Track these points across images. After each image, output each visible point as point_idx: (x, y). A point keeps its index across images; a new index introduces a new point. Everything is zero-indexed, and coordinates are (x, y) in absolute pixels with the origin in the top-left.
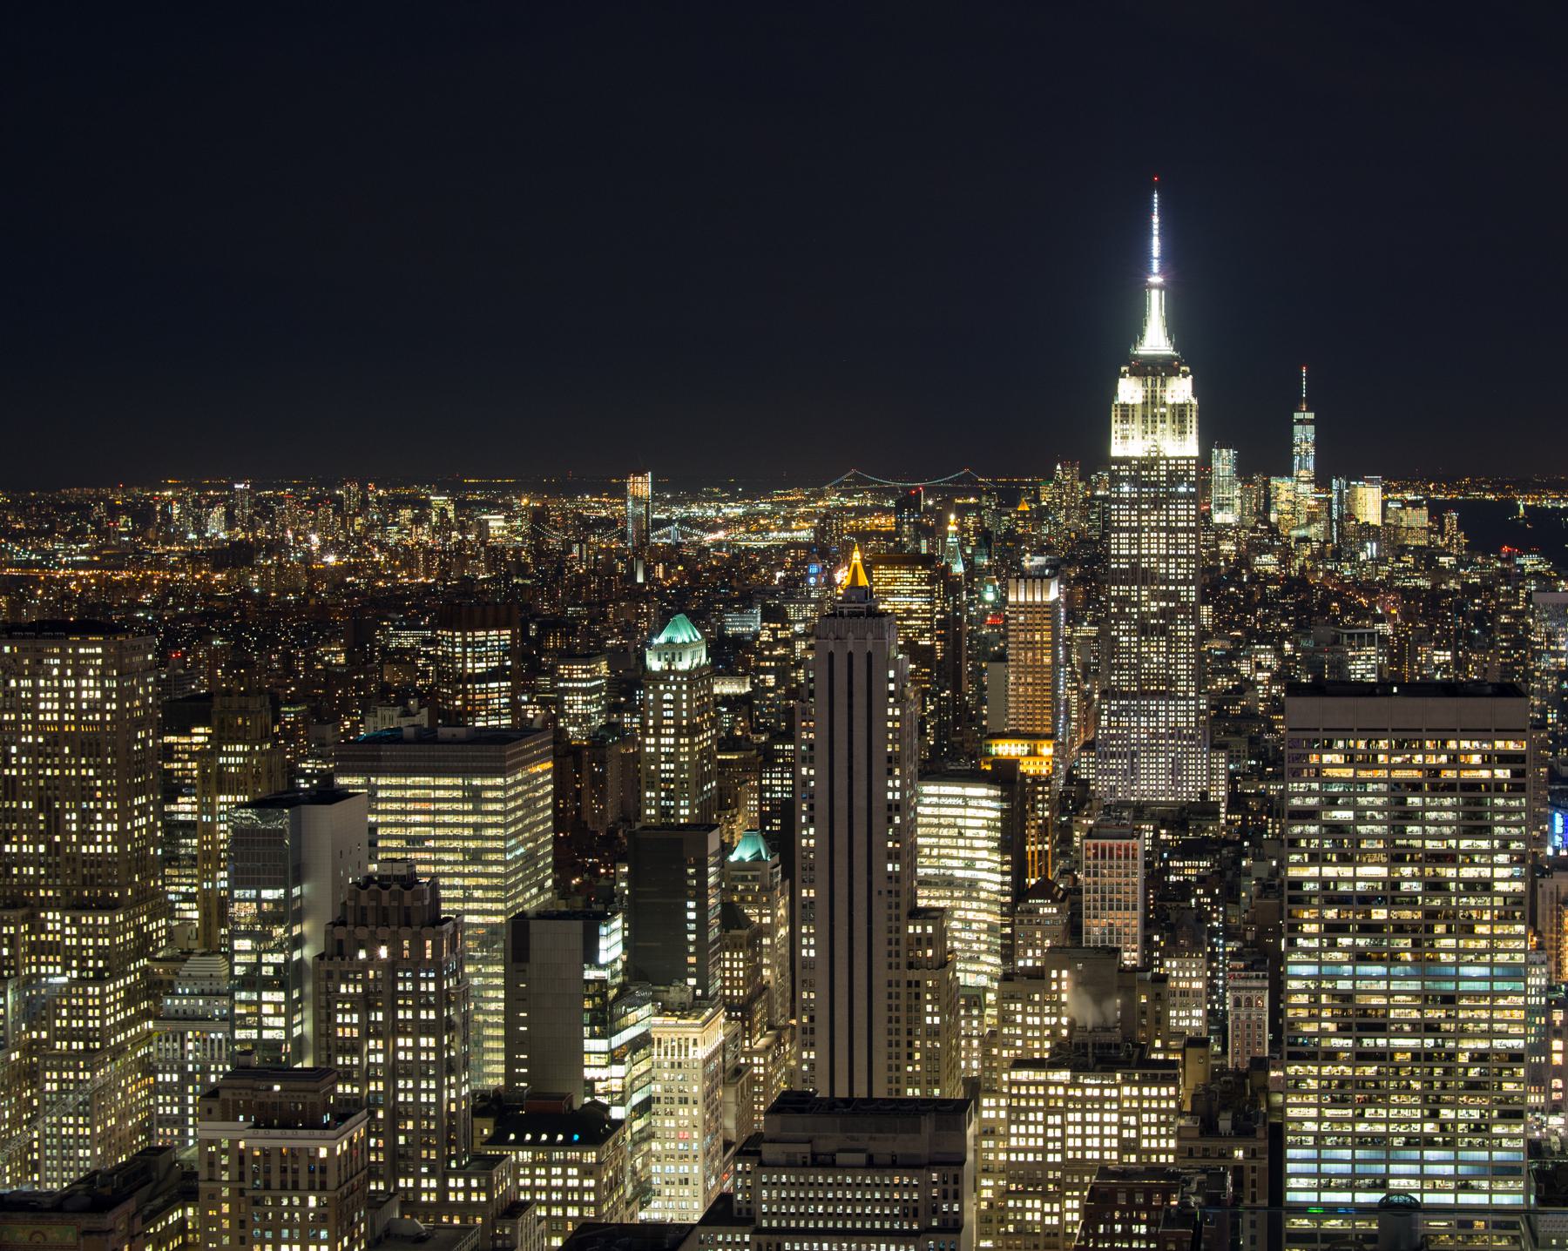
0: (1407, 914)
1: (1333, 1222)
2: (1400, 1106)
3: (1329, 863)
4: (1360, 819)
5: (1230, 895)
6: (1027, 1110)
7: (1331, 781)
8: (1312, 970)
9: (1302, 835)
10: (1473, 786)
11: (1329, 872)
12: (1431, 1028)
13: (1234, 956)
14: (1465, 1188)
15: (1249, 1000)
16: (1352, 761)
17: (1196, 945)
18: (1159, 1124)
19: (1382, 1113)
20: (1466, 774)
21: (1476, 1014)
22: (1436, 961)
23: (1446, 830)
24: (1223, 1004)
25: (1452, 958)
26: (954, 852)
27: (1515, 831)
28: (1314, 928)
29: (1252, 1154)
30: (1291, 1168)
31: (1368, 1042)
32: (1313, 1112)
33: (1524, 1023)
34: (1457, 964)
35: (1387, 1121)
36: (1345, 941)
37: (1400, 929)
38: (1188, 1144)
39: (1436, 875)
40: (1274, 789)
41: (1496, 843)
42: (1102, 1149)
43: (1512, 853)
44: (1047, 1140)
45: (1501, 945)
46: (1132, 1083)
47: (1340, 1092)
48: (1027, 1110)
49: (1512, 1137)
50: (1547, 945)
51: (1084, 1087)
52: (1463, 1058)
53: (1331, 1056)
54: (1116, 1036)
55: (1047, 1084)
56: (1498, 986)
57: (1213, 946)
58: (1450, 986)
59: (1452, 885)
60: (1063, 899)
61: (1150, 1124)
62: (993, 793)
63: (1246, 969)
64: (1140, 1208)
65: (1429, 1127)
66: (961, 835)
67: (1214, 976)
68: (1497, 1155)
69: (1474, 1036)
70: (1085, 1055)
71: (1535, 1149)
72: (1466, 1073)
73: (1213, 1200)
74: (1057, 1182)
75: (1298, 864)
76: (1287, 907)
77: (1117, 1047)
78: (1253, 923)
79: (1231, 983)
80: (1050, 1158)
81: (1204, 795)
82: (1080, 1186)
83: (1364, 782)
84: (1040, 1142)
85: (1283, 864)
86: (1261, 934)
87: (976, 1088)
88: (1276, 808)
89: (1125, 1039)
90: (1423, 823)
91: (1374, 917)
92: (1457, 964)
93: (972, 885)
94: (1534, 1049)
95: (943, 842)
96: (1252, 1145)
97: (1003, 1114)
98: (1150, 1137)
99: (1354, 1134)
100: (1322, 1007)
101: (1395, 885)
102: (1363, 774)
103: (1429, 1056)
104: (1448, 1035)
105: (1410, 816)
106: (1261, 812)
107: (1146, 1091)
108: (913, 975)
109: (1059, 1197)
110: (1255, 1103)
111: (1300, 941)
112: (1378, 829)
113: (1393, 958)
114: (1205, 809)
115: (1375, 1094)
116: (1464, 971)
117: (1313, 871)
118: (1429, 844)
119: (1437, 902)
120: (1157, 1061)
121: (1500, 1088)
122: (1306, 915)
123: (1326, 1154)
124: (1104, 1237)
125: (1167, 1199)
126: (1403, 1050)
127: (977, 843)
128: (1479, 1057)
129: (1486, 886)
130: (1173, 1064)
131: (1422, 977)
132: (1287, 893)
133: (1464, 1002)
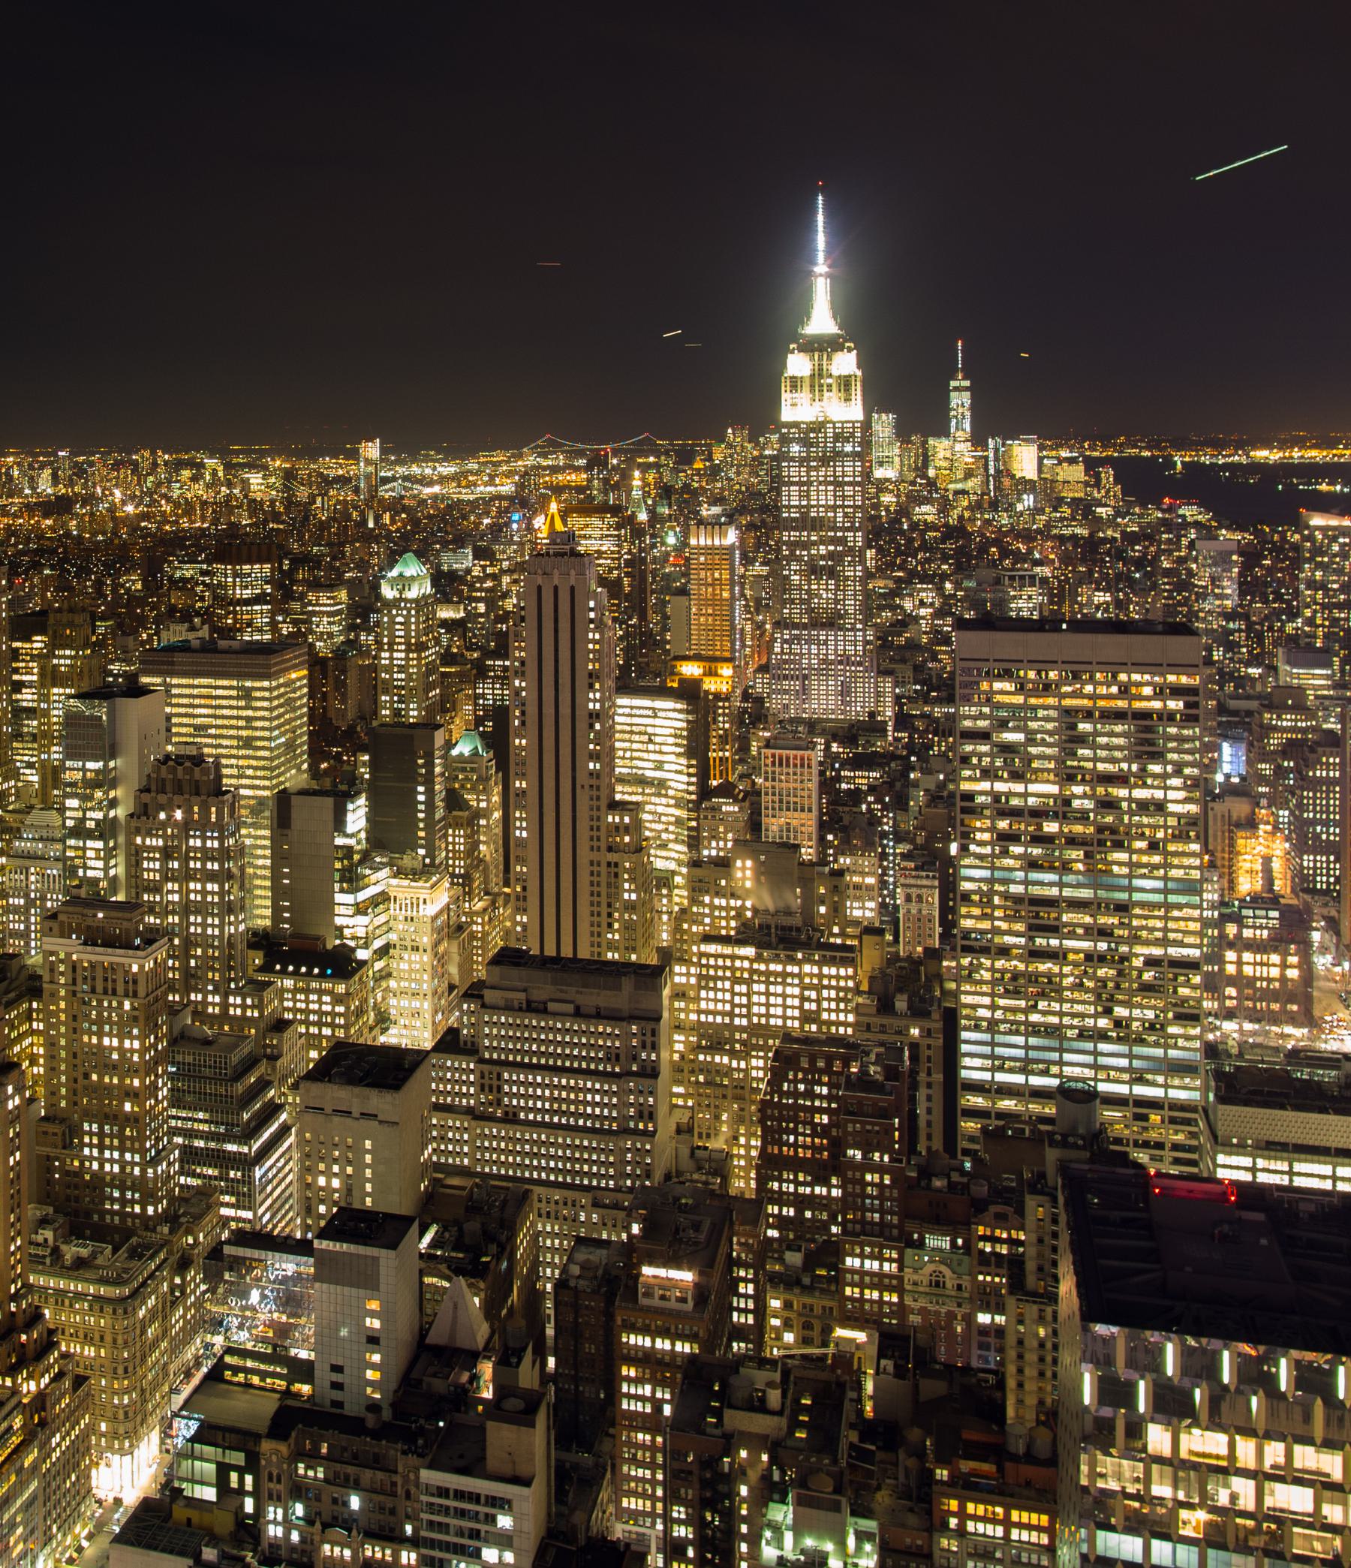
0: (1078, 829)
1: (1007, 1102)
2: (1073, 1001)
3: (1001, 779)
4: (1031, 741)
5: (900, 803)
6: (716, 978)
7: (1000, 706)
8: (985, 874)
9: (974, 753)
10: (1146, 715)
11: (1000, 787)
12: (1104, 933)
13: (904, 856)
14: (1140, 1080)
15: (920, 897)
16: (1022, 688)
17: (869, 845)
18: (838, 1000)
19: (1055, 1006)
20: (1137, 705)
21: (1151, 923)
22: (1108, 872)
23: (1118, 754)
24: (894, 898)
25: (1125, 870)
26: (645, 755)
27: (1188, 758)
28: (986, 836)
29: (927, 1033)
30: (965, 1048)
31: (1040, 941)
32: (987, 1001)
33: (1201, 934)
34: (1130, 876)
35: (1061, 1014)
36: (1017, 850)
37: (1072, 841)
38: (866, 1019)
39: (1107, 794)
40: (938, 711)
41: (1169, 768)
42: (784, 1017)
43: (1186, 778)
44: (734, 1005)
45: (1176, 861)
46: (813, 962)
47: (1013, 985)
48: (716, 978)
49: (1188, 1038)
50: (1219, 863)
51: (767, 962)
52: (1138, 962)
53: (1004, 952)
54: (797, 921)
55: (733, 957)
56: (1172, 898)
57: (884, 847)
58: (1124, 896)
59: (1124, 805)
60: (744, 800)
61: (829, 1000)
62: (679, 706)
63: (916, 869)
64: (821, 1072)
65: (1103, 1023)
66: (650, 741)
67: (884, 874)
68: (1172, 1053)
69: (1147, 943)
70: (769, 935)
71: (1212, 1050)
72: (1140, 976)
73: (891, 1073)
74: (743, 1043)
75: (970, 779)
76: (959, 816)
77: (798, 930)
78: (923, 829)
79: (902, 880)
80: (737, 1021)
81: (872, 715)
82: (766, 1048)
83: (1035, 708)
84: (728, 1007)
85: (953, 777)
86: (931, 838)
87: (667, 957)
88: (946, 728)
89: (805, 924)
90: (1094, 747)
91: (1046, 829)
92: (1130, 876)
93: (662, 784)
94: (1209, 959)
95: (635, 746)
96: (928, 1025)
97: (693, 980)
98: (829, 1010)
99: (1027, 1023)
100: (995, 907)
101: (1067, 802)
102: (1033, 701)
103: (1102, 959)
104: (1120, 941)
105: (1082, 740)
106: (926, 731)
107: (825, 970)
108: (613, 857)
109: (746, 1056)
110: (929, 989)
111: (972, 848)
112: (1049, 751)
113: (1065, 867)
114: (873, 726)
115: (1050, 988)
116: (1138, 883)
117: (985, 786)
118: (1100, 766)
119: (1109, 819)
120: (834, 945)
121: (1175, 992)
122: (978, 824)
123: (998, 1038)
124: (788, 1094)
125: (846, 1065)
126: (1076, 951)
127: (665, 749)
128: (1151, 962)
129: (1160, 807)
130: (851, 949)
131: (1096, 886)
132: (959, 804)
133: (1137, 911)
